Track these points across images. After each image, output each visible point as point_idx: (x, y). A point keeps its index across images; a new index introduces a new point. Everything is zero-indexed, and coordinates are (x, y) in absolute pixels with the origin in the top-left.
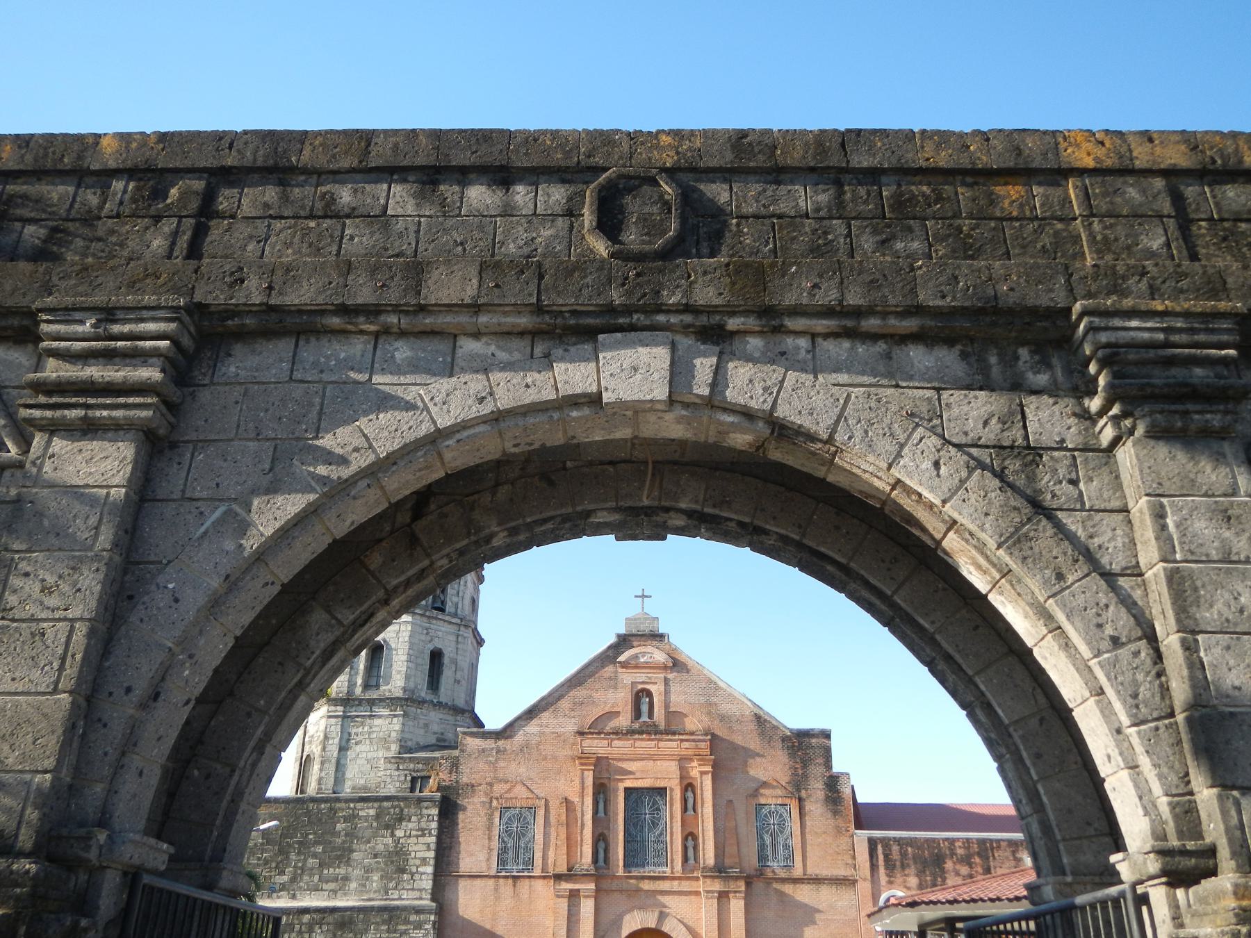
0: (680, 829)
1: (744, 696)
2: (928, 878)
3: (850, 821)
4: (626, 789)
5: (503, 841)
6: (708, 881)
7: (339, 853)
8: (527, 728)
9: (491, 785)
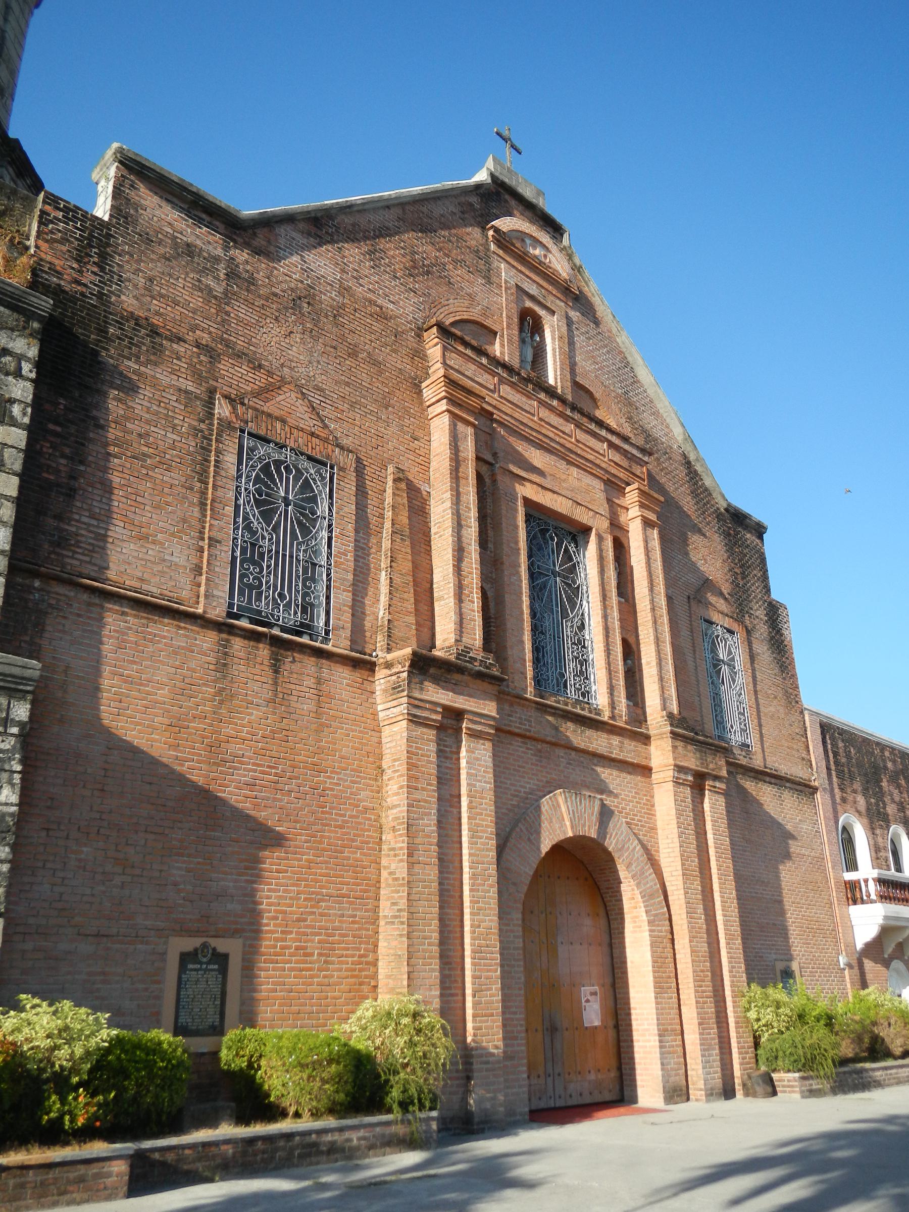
2: (873, 801)
4: (527, 501)
5: (248, 527)
8: (310, 256)
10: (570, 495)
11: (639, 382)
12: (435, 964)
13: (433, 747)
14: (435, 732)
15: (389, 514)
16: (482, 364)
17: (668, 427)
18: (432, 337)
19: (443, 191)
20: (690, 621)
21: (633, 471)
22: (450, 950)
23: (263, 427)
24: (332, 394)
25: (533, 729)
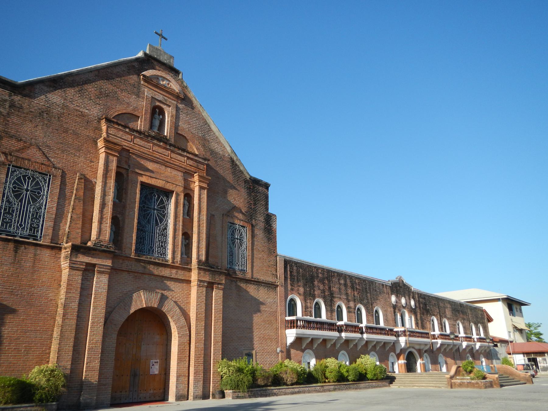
0: (181, 227)
2: (308, 289)
4: (143, 184)
5: (8, 201)
6: (202, 273)
8: (49, 95)
10: (164, 179)
11: (212, 130)
12: (71, 354)
13: (80, 277)
14: (82, 272)
15: (75, 192)
16: (126, 131)
17: (224, 147)
18: (103, 122)
19: (118, 63)
20: (222, 224)
21: (199, 167)
22: (80, 348)
23: (20, 162)
24: (54, 148)
25: (132, 269)
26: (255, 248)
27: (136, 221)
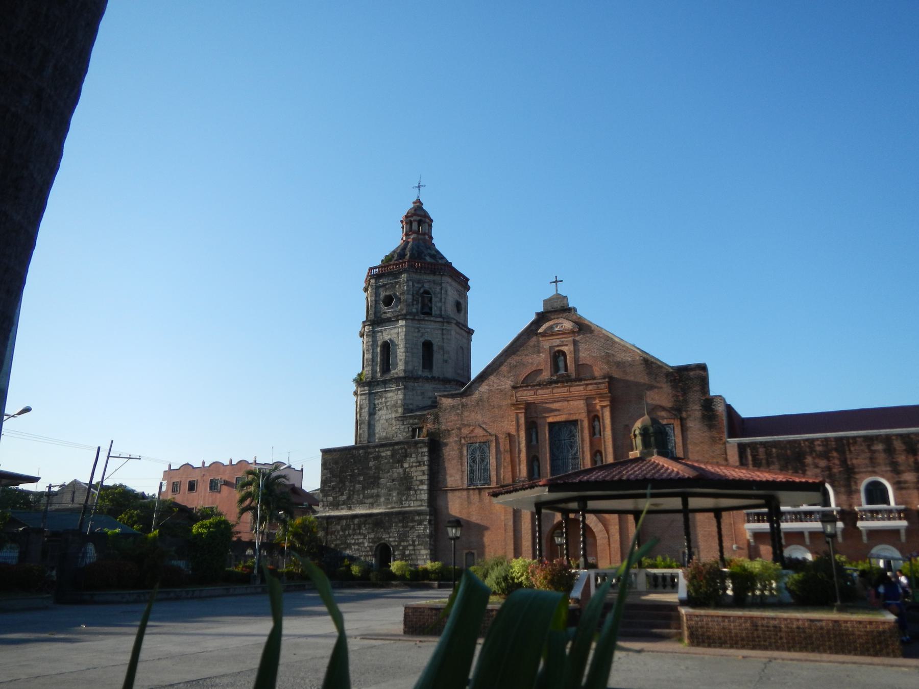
0: (588, 448)
1: (634, 346)
3: (723, 432)
5: (470, 466)
7: (372, 480)
9: (460, 429)
10: (566, 413)
17: (634, 351)
21: (600, 388)
26: (688, 442)
27: (548, 455)
